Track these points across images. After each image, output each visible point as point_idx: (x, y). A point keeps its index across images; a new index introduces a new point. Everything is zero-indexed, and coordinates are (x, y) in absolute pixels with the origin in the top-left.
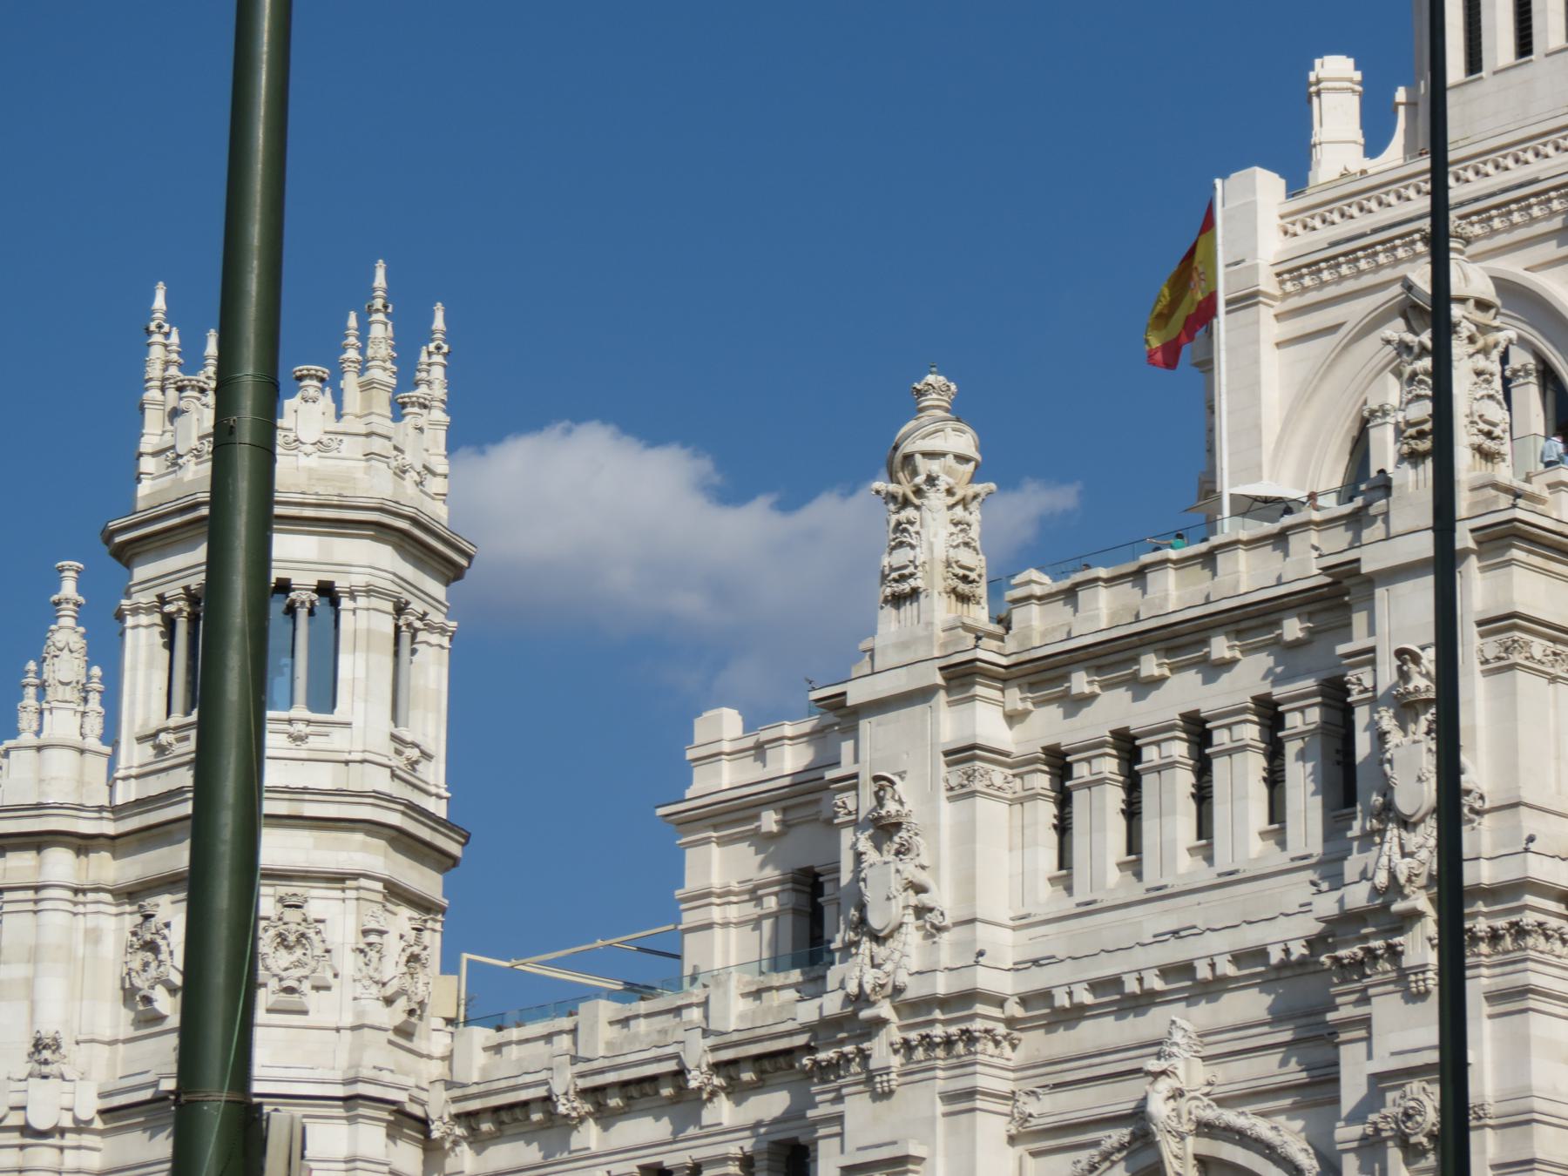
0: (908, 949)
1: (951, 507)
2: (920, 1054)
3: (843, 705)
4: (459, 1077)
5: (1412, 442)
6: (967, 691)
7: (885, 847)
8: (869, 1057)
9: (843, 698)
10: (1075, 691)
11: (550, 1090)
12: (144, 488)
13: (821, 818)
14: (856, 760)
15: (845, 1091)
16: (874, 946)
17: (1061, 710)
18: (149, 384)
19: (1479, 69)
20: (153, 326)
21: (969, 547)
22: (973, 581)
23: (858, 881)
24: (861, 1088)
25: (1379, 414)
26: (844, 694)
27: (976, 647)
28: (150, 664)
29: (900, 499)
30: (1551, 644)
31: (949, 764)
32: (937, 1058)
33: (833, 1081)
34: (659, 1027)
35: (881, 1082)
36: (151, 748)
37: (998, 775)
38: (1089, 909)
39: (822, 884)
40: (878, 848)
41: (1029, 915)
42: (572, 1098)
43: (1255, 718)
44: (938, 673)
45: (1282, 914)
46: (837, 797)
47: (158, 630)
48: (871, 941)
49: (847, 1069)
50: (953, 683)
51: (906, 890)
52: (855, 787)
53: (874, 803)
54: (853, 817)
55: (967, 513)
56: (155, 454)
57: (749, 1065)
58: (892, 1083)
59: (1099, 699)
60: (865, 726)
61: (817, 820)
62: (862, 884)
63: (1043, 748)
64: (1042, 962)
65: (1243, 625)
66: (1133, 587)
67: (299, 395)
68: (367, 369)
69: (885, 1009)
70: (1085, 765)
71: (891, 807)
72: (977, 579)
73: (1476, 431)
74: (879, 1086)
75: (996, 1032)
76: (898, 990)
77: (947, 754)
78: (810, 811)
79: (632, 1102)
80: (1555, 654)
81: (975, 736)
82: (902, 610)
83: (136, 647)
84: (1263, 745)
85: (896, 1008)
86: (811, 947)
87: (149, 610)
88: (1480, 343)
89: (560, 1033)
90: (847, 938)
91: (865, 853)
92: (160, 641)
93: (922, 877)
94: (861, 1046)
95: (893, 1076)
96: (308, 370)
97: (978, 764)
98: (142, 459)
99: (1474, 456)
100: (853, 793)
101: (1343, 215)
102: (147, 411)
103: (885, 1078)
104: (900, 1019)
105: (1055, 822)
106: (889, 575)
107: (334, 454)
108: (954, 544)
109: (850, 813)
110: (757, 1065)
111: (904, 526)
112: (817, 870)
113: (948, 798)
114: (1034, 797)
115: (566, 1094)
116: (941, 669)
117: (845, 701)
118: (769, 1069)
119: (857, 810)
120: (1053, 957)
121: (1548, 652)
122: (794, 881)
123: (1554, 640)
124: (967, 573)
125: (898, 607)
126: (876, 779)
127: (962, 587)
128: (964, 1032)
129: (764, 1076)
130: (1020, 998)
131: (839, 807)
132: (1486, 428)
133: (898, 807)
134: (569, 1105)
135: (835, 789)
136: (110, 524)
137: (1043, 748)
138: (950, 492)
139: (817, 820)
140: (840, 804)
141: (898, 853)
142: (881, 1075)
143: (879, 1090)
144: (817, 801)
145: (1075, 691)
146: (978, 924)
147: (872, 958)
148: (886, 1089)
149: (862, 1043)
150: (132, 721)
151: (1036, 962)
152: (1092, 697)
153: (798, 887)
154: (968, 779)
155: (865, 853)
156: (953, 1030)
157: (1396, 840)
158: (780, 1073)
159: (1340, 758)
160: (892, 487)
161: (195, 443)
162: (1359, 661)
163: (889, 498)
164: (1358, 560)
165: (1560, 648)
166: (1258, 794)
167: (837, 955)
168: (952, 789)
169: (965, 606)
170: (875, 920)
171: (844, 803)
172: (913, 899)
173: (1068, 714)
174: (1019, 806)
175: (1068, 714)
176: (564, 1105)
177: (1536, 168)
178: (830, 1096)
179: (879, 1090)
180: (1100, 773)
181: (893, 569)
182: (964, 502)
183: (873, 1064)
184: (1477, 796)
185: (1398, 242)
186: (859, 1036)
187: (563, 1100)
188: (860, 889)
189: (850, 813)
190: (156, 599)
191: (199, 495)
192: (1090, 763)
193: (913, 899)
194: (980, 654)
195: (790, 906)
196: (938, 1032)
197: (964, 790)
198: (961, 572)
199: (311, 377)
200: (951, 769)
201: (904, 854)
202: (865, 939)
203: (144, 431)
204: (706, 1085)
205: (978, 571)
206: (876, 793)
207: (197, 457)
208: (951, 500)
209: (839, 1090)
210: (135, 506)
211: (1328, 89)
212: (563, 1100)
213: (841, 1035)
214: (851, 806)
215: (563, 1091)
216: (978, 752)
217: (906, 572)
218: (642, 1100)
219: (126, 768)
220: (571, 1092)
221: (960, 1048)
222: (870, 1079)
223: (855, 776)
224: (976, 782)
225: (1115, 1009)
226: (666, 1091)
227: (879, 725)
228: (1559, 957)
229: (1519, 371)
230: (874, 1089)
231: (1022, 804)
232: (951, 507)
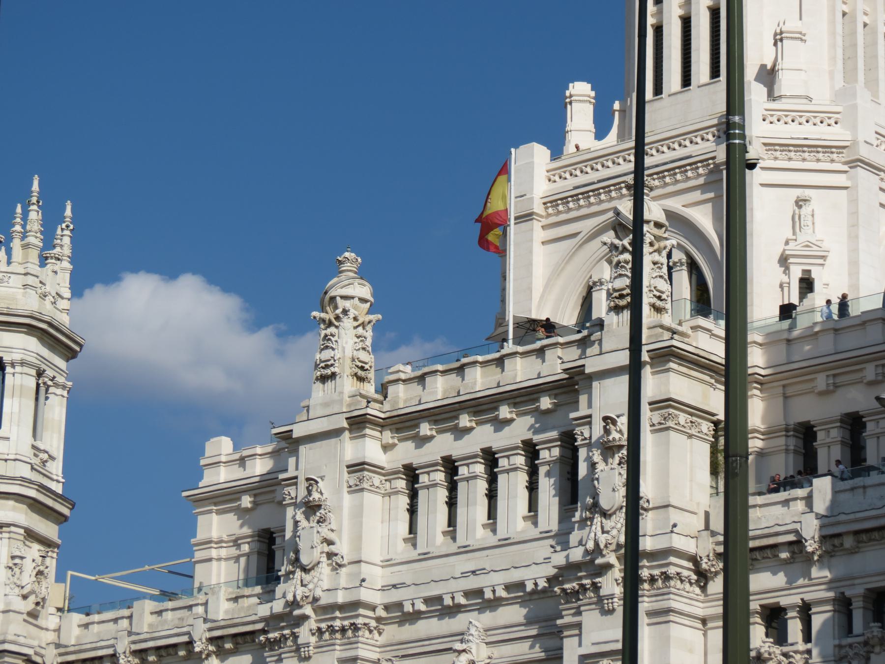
0: (322, 577)
1: (356, 328)
2: (327, 636)
3: (290, 437)
4: (63, 641)
5: (616, 300)
6: (361, 432)
7: (311, 518)
8: (298, 636)
10: (422, 434)
11: (115, 650)
13: (276, 501)
14: (297, 469)
15: (283, 656)
16: (303, 574)
17: (414, 444)
19: (661, 93)
21: (365, 351)
22: (367, 370)
23: (295, 537)
24: (293, 654)
25: (598, 284)
26: (291, 431)
27: (367, 407)
29: (327, 322)
30: (690, 417)
31: (349, 473)
32: (336, 639)
33: (277, 650)
34: (179, 616)
35: (304, 652)
37: (377, 480)
38: (425, 557)
39: (274, 538)
40: (308, 519)
41: (391, 560)
42: (128, 655)
43: (523, 453)
45: (534, 563)
46: (285, 489)
48: (301, 571)
49: (285, 643)
50: (354, 427)
51: (322, 543)
52: (296, 484)
53: (306, 493)
54: (294, 501)
55: (364, 331)
57: (230, 639)
58: (310, 652)
59: (435, 438)
60: (303, 449)
61: (273, 501)
62: (297, 539)
63: (403, 465)
64: (397, 586)
65: (518, 400)
66: (457, 376)
68: (27, 237)
69: (308, 610)
70: (426, 476)
71: (316, 495)
72: (369, 368)
73: (652, 296)
74: (303, 653)
75: (370, 625)
76: (316, 600)
77: (348, 467)
79: (161, 659)
80: (691, 422)
82: (326, 385)
84: (526, 468)
85: (314, 610)
86: (267, 573)
88: (656, 247)
89: (123, 618)
90: (288, 569)
91: (300, 521)
93: (331, 536)
94: (293, 630)
95: (311, 648)
97: (366, 473)
100: (295, 487)
101: (582, 172)
103: (306, 649)
104: (316, 616)
105: (408, 507)
106: (319, 365)
107: (6, 284)
109: (292, 498)
110: (234, 639)
112: (272, 530)
113: (348, 492)
114: (397, 493)
115: (125, 653)
116: (347, 419)
118: (241, 642)
119: (296, 497)
120: (404, 583)
121: (688, 421)
122: (259, 536)
123: (691, 414)
124: (363, 365)
125: (324, 383)
126: (308, 479)
127: (360, 373)
128: (352, 624)
129: (238, 646)
130: (384, 606)
131: (286, 495)
132: (658, 294)
133: (320, 496)
134: (126, 659)
135: (284, 484)
137: (403, 465)
138: (355, 319)
139: (273, 501)
140: (287, 493)
141: (318, 522)
142: (304, 648)
143: (303, 656)
144: (273, 491)
145: (422, 434)
146: (362, 563)
147: (302, 581)
148: (307, 655)
149: (294, 629)
151: (394, 586)
152: (432, 437)
153: (261, 539)
154: (359, 481)
155: (300, 521)
156: (346, 623)
157: (599, 524)
158: (247, 644)
159: (569, 476)
160: (323, 315)
162: (582, 422)
163: (321, 321)
164: (584, 366)
165: (694, 419)
166: (523, 496)
167: (282, 579)
168: (350, 487)
169: (362, 383)
170: (304, 560)
171: (289, 492)
172: (326, 548)
173: (418, 447)
174: (388, 497)
175: (418, 447)
176: (123, 659)
177: (691, 149)
178: (275, 658)
179: (303, 656)
180: (435, 480)
181: (321, 361)
182: (363, 325)
183: (300, 641)
184: (646, 500)
185: (612, 188)
186: (294, 625)
187: (122, 656)
188: (297, 543)
189: (292, 498)
192: (429, 474)
193: (326, 548)
194: (369, 411)
195: (256, 550)
196: (337, 624)
197: (357, 488)
198: (360, 364)
200: (350, 475)
201: (322, 523)
202: (298, 570)
204: (204, 650)
205: (369, 364)
206: (307, 488)
208: (356, 324)
209: (280, 655)
212: (122, 656)
213: (282, 624)
214: (293, 495)
215: (123, 651)
216: (366, 466)
217: (329, 363)
218: (167, 658)
220: (128, 652)
221: (350, 633)
222: (298, 650)
223: (296, 478)
224: (364, 483)
225: (438, 614)
226: (182, 653)
227: (310, 449)
228: (688, 592)
230: (300, 655)
231: (390, 496)
232: (356, 328)
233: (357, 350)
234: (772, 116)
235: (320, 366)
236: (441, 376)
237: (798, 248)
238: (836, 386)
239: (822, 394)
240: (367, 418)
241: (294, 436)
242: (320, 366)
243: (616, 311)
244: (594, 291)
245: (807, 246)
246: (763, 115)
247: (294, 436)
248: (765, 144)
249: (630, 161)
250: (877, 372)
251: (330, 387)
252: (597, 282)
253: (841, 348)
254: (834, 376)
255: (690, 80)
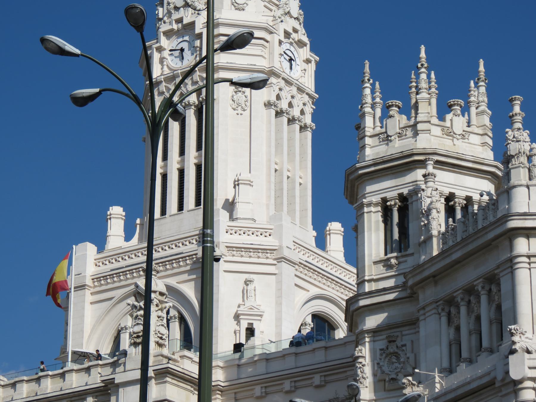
1: (156, 311)
3: (113, 383)
9: (113, 380)
12: (368, 151)
18: (365, 105)
19: (165, 214)
20: (419, 65)
25: (173, 318)
26: (114, 378)
27: (168, 363)
28: (377, 229)
29: (138, 308)
36: (382, 267)
44: (152, 372)
47: (380, 214)
50: (158, 376)
55: (162, 314)
56: (371, 137)
60: (121, 390)
61: (282, 391)
66: (85, 373)
67: (452, 113)
78: (280, 387)
81: (166, 396)
82: (137, 348)
83: (370, 221)
87: (376, 205)
88: (160, 307)
92: (381, 219)
96: (457, 101)
98: (418, 125)
99: (156, 345)
101: (162, 249)
102: (419, 103)
106: (132, 335)
107: (466, 140)
108: (158, 325)
111: (139, 317)
116: (153, 370)
117: (114, 381)
124: (162, 336)
125: (135, 347)
127: (161, 341)
136: (357, 165)
138: (157, 305)
150: (370, 255)
160: (136, 303)
161: (398, 131)
169: (161, 348)
177: (182, 249)
181: (134, 333)
182: (161, 310)
185: (134, 271)
190: (380, 200)
191: (414, 150)
194: (170, 366)
198: (160, 336)
199: (458, 105)
203: (418, 112)
205: (166, 335)
207: (399, 137)
210: (365, 158)
211: (241, 183)
219: (368, 276)
229: (173, 317)
232: (156, 311)
233: (158, 326)
234: (232, 230)
235: (133, 336)
236: (26, 383)
237: (246, 309)
238: (327, 382)
239: (317, 387)
240: (168, 370)
241: (116, 382)
242: (133, 336)
243: (135, 345)
244: (171, 322)
245: (251, 309)
246: (226, 229)
247: (116, 382)
248: (227, 247)
249: (193, 243)
250: (292, 385)
251: (137, 351)
252: (173, 317)
253: (329, 358)
254: (325, 376)
255: (183, 207)
